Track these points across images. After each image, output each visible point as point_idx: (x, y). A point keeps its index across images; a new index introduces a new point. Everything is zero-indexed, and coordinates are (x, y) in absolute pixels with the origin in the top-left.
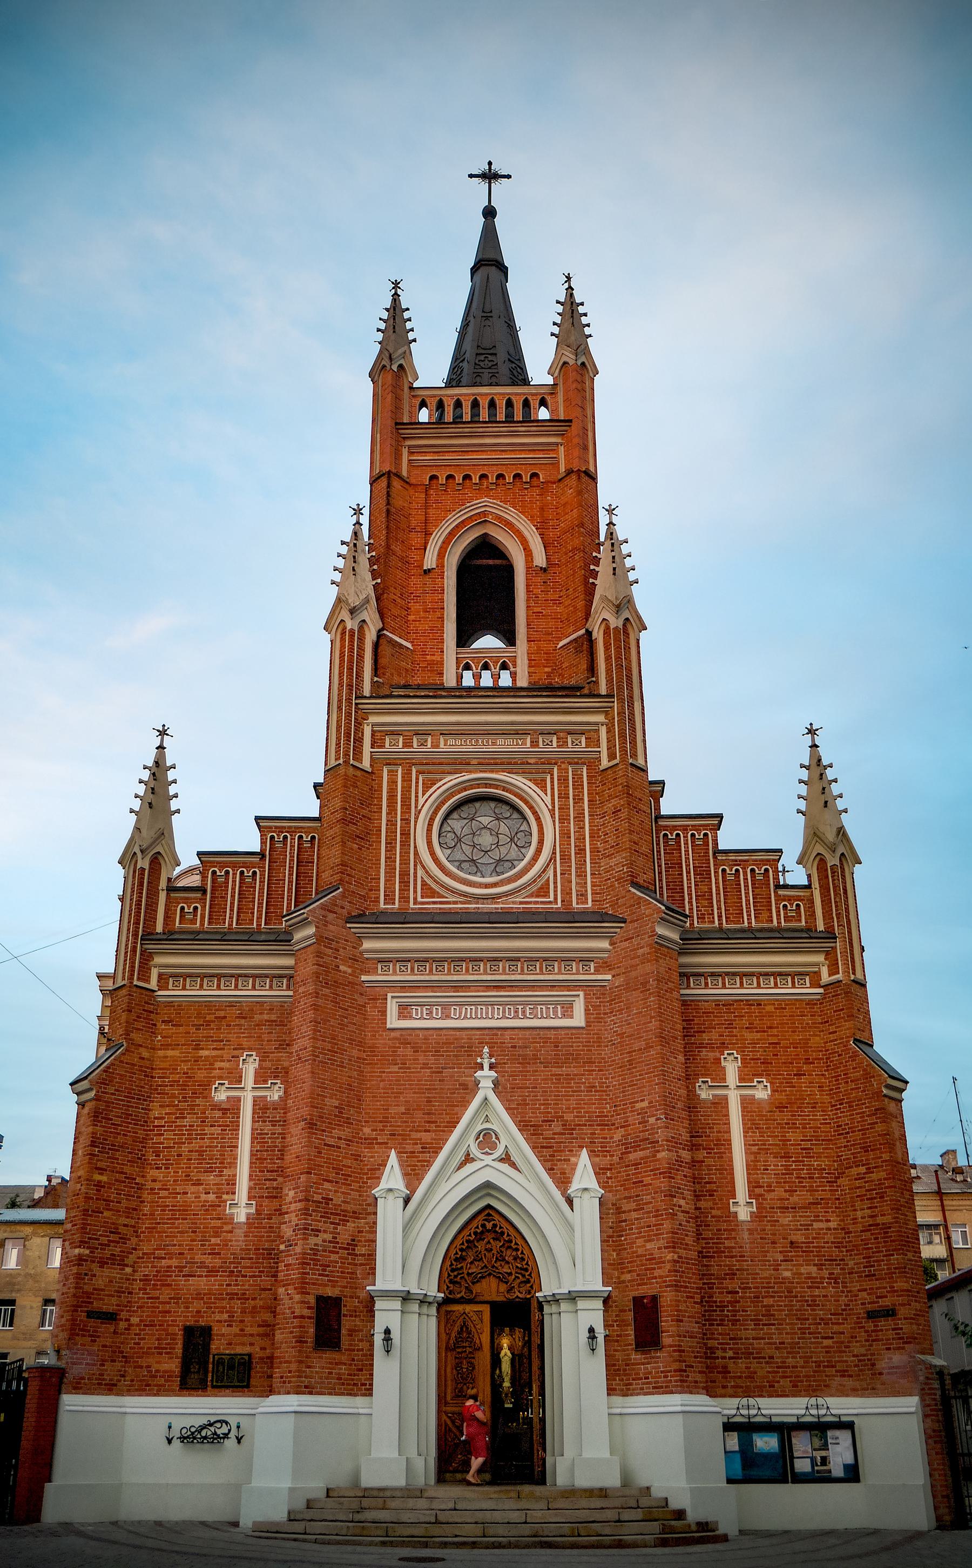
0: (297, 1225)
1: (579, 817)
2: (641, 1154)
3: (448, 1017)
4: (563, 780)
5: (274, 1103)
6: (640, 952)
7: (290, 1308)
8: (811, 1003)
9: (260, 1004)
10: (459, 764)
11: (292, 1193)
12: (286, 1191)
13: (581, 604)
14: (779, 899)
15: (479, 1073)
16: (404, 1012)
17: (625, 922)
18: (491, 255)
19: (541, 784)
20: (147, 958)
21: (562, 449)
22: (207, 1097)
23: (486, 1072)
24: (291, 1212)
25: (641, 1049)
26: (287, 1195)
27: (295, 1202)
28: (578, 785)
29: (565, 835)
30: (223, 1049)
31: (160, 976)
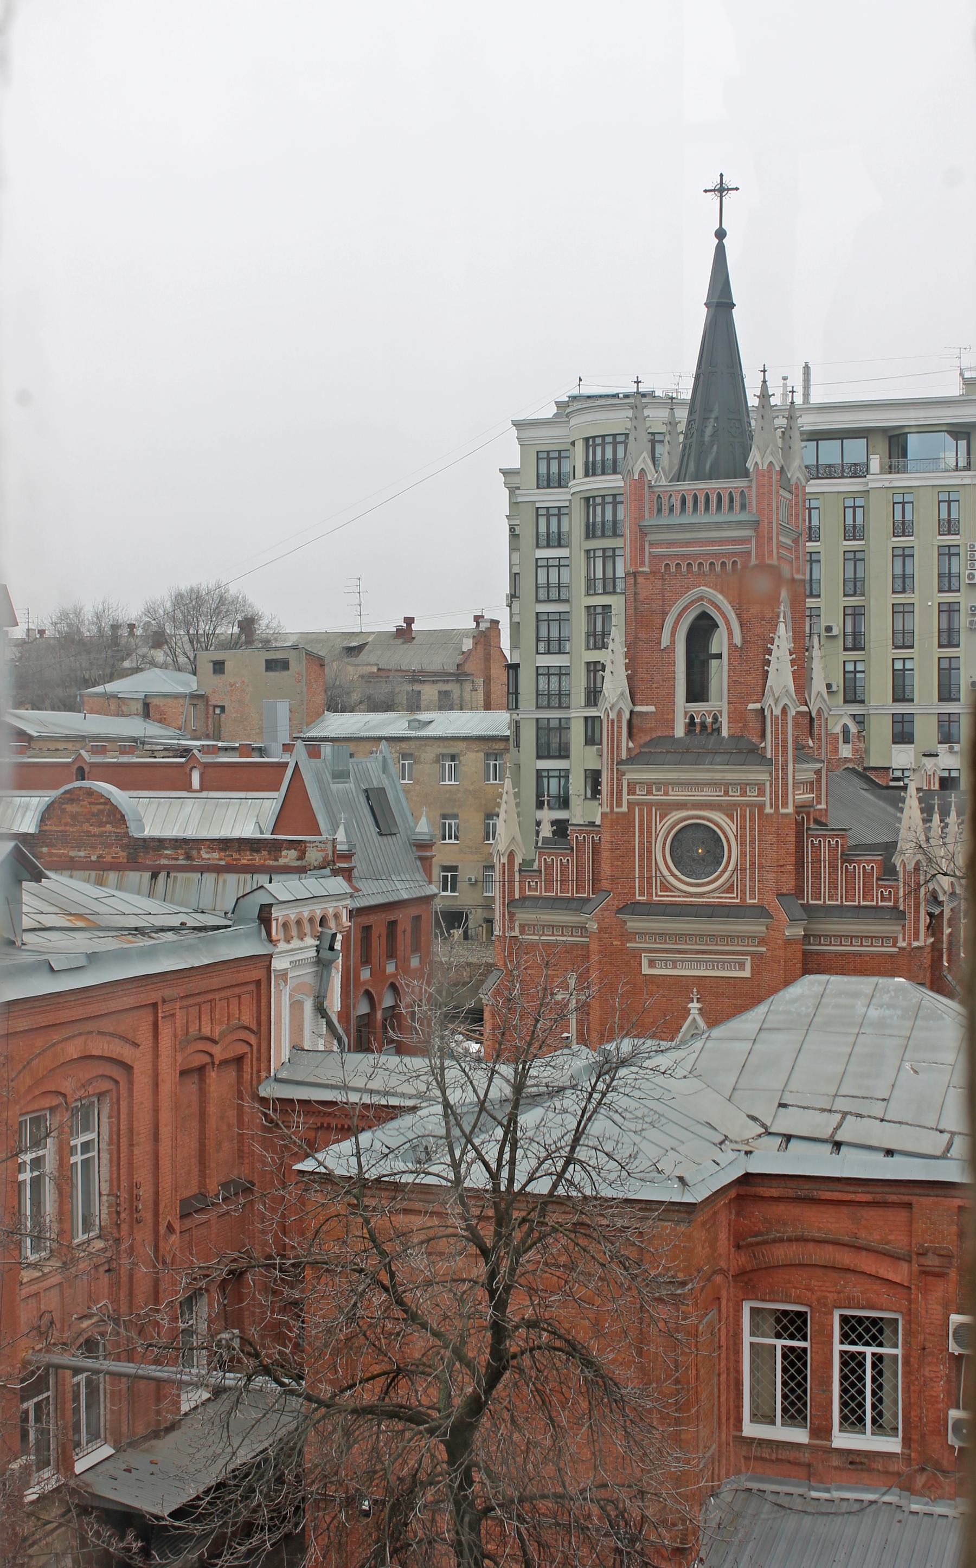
1: (752, 841)
3: (675, 967)
4: (743, 817)
8: (891, 956)
9: (576, 944)
10: (681, 806)
13: (760, 682)
14: (879, 887)
15: (690, 1005)
16: (652, 964)
19: (731, 817)
20: (512, 915)
21: (754, 540)
28: (752, 819)
29: (743, 854)
31: (520, 925)
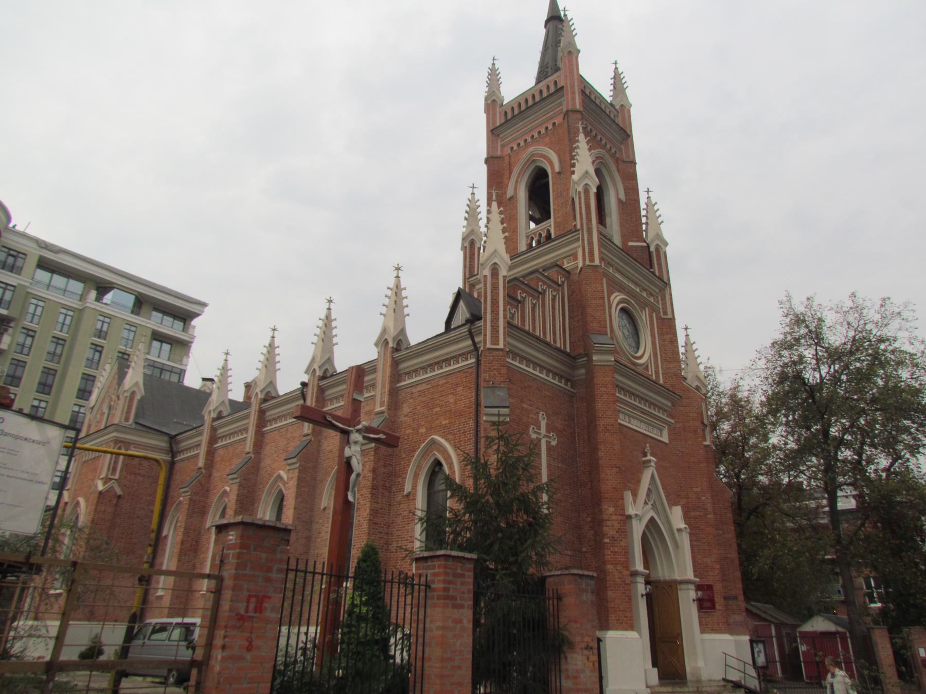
0: (619, 529)
2: (698, 514)
3: (629, 422)
5: (553, 446)
6: (691, 415)
7: (619, 578)
10: (622, 288)
11: (612, 509)
12: (605, 506)
17: (681, 397)
18: (556, 15)
22: (528, 434)
23: (649, 457)
24: (613, 520)
25: (694, 462)
26: (608, 509)
27: (616, 515)
30: (531, 406)
